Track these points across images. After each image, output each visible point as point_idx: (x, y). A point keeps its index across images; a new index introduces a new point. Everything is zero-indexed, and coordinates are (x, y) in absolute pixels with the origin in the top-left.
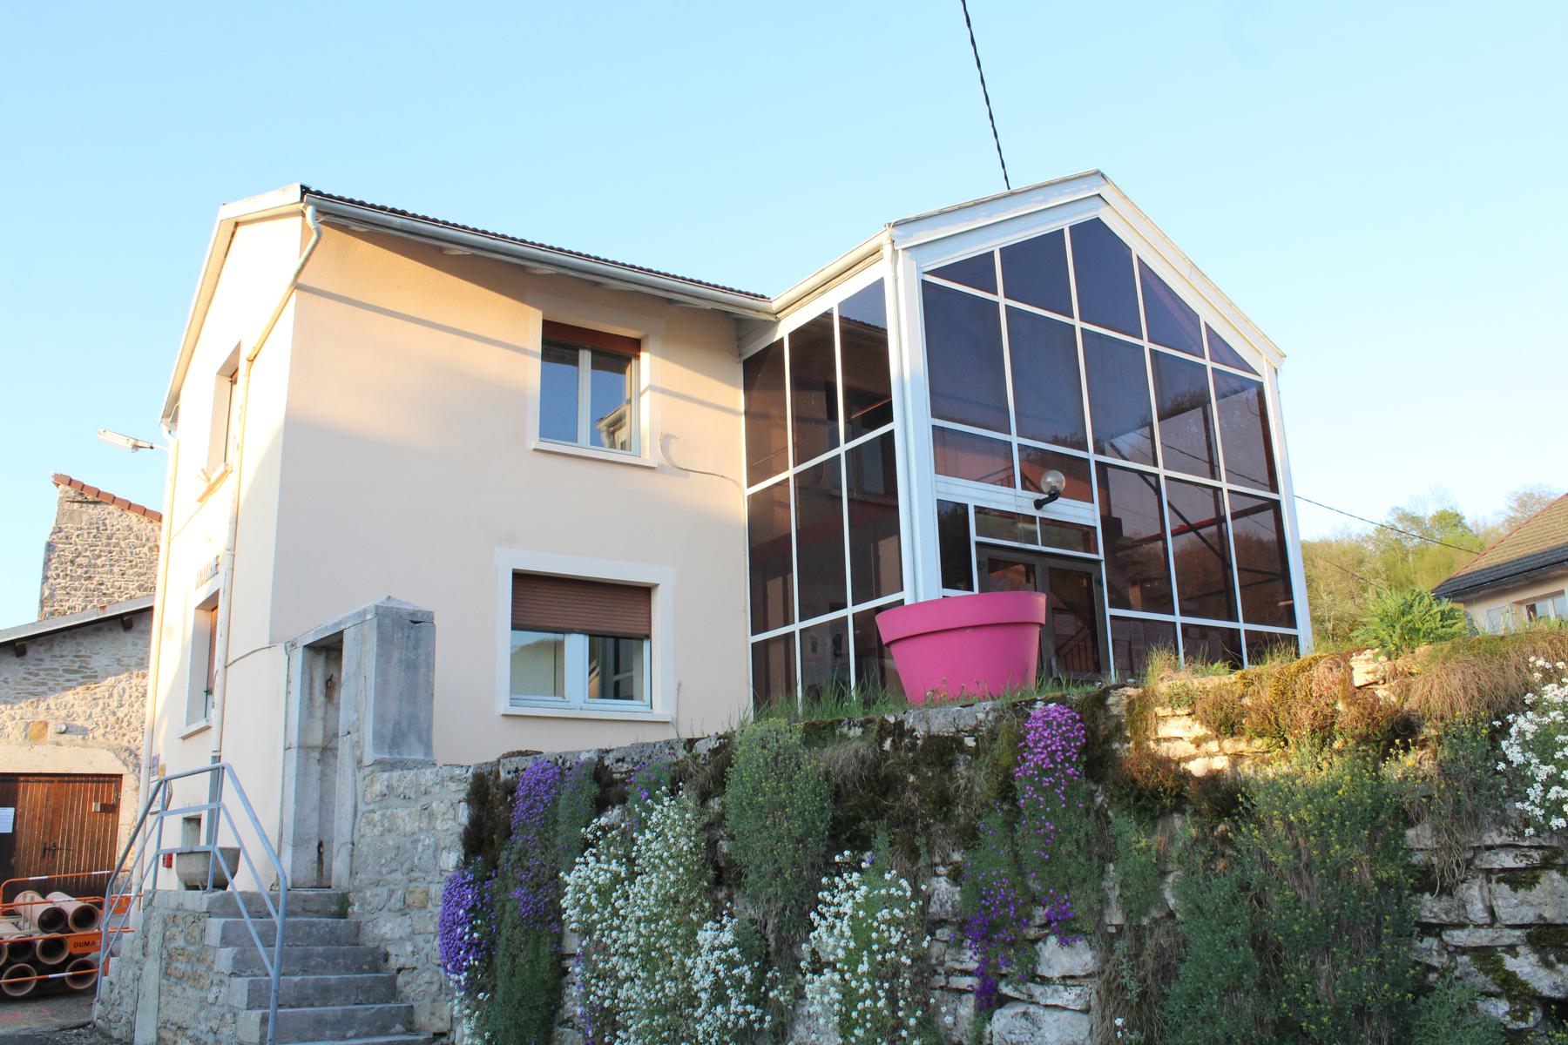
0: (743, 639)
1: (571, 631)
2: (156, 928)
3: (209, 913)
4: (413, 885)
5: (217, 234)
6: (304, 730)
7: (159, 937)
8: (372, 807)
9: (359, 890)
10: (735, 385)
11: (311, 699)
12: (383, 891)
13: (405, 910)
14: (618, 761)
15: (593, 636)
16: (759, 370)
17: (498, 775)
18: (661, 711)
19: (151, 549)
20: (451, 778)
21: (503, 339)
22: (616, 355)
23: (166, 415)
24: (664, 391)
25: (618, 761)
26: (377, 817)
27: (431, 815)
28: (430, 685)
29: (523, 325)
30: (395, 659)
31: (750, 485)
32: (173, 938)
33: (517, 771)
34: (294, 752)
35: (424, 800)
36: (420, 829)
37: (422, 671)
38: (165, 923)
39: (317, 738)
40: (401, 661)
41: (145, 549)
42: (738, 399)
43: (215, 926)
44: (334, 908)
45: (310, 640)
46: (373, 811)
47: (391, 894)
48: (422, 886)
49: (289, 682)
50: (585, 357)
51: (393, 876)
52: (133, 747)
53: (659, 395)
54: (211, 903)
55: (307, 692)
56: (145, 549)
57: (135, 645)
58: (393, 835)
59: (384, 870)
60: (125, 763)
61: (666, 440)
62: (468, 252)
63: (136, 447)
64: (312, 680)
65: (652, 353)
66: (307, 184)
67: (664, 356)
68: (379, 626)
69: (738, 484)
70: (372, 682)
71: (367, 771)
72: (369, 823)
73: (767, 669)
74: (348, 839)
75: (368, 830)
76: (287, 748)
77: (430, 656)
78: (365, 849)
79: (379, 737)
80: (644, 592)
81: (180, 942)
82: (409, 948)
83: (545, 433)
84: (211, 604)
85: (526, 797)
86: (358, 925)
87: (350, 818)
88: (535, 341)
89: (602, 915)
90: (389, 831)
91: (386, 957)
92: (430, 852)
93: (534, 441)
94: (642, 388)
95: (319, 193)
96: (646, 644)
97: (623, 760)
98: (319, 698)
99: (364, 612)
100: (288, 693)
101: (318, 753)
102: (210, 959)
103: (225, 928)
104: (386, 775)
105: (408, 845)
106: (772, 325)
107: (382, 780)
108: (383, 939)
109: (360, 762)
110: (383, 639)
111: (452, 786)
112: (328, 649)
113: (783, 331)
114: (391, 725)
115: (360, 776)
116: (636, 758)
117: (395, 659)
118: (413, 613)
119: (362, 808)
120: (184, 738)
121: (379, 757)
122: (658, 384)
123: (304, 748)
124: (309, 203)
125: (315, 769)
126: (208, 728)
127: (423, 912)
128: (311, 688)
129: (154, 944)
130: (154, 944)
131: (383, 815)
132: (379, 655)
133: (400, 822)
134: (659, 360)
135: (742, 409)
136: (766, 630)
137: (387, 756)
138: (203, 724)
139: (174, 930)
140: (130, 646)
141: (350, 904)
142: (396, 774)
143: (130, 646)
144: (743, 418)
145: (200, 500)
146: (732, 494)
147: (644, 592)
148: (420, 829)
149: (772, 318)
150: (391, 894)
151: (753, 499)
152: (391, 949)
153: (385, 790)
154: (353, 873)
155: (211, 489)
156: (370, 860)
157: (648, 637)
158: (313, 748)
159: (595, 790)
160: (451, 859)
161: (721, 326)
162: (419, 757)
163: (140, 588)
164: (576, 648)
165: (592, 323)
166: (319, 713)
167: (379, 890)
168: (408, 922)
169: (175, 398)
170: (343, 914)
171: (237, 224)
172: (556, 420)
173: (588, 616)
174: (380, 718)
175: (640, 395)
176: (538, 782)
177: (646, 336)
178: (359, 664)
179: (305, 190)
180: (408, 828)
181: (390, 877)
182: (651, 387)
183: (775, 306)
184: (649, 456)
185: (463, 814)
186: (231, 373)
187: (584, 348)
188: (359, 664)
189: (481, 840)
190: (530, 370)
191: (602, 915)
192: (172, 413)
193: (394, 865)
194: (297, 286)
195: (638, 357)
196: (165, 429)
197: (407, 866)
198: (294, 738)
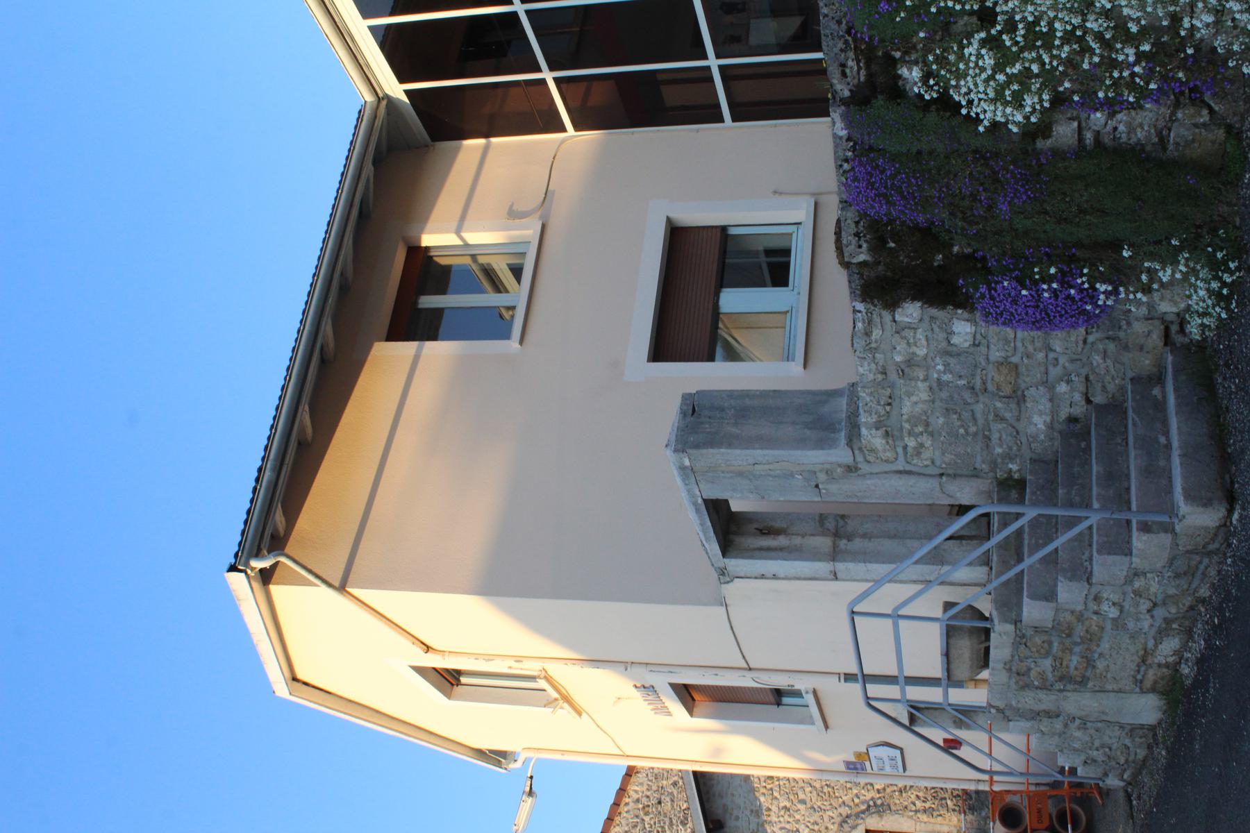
0: (728, 135)
1: (716, 306)
2: (1029, 700)
3: (1017, 622)
4: (990, 387)
5: (303, 701)
6: (815, 556)
7: (1041, 695)
8: (900, 450)
9: (994, 465)
10: (458, 149)
11: (781, 549)
12: (996, 427)
13: (1018, 397)
14: (844, 75)
15: (721, 284)
16: (445, 120)
17: (863, 264)
18: (800, 212)
19: (647, 814)
20: (868, 334)
21: (403, 380)
22: (426, 272)
23: (499, 764)
24: (463, 218)
25: (844, 75)
26: (911, 443)
27: (910, 362)
28: (764, 394)
29: (390, 361)
30: (734, 430)
31: (563, 129)
32: (1042, 675)
33: (857, 235)
34: (840, 567)
35: (893, 376)
36: (925, 380)
37: (748, 402)
38: (1024, 687)
39: (824, 543)
40: (736, 424)
41: (647, 819)
42: (473, 144)
43: (1034, 611)
44: (1014, 494)
45: (715, 548)
46: (905, 447)
47: (999, 418)
48: (991, 372)
49: (763, 577)
50: (429, 301)
51: (979, 416)
52: (839, 820)
53: (466, 224)
54: (1005, 619)
55: (773, 554)
56: (647, 819)
57: (737, 818)
58: (932, 420)
59: (973, 429)
60: (854, 827)
61: (514, 214)
62: (305, 408)
63: (531, 793)
64: (761, 549)
65: (421, 232)
66: (227, 567)
67: (426, 220)
68: (697, 446)
69: (563, 141)
70: (758, 454)
71: (860, 458)
72: (919, 454)
73: (762, 100)
74: (933, 483)
75: (926, 454)
76: (835, 577)
77: (731, 394)
78: (949, 457)
79: (821, 444)
80: (676, 235)
81: (1047, 663)
82: (1063, 388)
83: (506, 335)
84: (687, 694)
85: (888, 203)
86: (1033, 461)
87: (912, 480)
88: (407, 348)
89: (1032, 61)
90: (927, 425)
91: (1072, 420)
92: (952, 361)
93: (513, 344)
94: (460, 243)
95: (236, 555)
96: (733, 231)
97: (843, 65)
98: (782, 541)
99: (682, 468)
100: (775, 577)
101: (838, 534)
102: (1069, 617)
103: (1034, 597)
104: (864, 431)
105: (944, 395)
106: (391, 102)
107: (873, 438)
108: (1050, 427)
109: (851, 469)
110: (712, 442)
111: (876, 333)
112: (729, 528)
113: (396, 89)
114: (808, 432)
115: (865, 468)
116: (841, 45)
117: (734, 430)
118: (684, 414)
119: (901, 465)
120: (827, 727)
121: (843, 441)
122: (455, 224)
123: (835, 555)
124: (247, 564)
125: (858, 543)
126: (815, 692)
127: (1022, 369)
128: (769, 549)
129: (1047, 701)
130: (1047, 701)
131: (910, 434)
132: (730, 446)
133: (918, 409)
134: (429, 225)
135: (482, 141)
136: (718, 106)
137: (843, 434)
138: (810, 699)
139: (1033, 674)
140: (739, 823)
141: (1010, 478)
142: (863, 418)
143: (739, 823)
144: (495, 140)
145: (580, 714)
146: (574, 142)
147: (676, 235)
148: (925, 380)
149: (384, 103)
150: (999, 418)
151: (577, 127)
152: (1064, 413)
153: (880, 433)
154: (975, 474)
155: (567, 699)
156: (961, 450)
157: (724, 229)
158: (835, 546)
159: (880, 101)
160: (963, 329)
161: (392, 163)
162: (843, 402)
163: (684, 824)
164: (733, 300)
165: (381, 286)
166: (797, 541)
167: (995, 436)
168: (1033, 390)
169: (480, 754)
170: (1021, 484)
171: (295, 679)
172: (493, 325)
173: (699, 284)
174: (801, 443)
175: (466, 245)
176: (871, 185)
177: (405, 240)
178: (740, 474)
179: (233, 568)
180: (924, 396)
181: (981, 421)
182: (458, 232)
183: (369, 98)
184: (528, 232)
185: (911, 312)
186: (449, 680)
187: (416, 303)
188: (740, 474)
189: (942, 290)
190: (438, 351)
191: (1032, 61)
192: (498, 757)
193: (966, 415)
194: (342, 588)
195: (427, 249)
196: (512, 766)
197: (967, 396)
198: (823, 567)
